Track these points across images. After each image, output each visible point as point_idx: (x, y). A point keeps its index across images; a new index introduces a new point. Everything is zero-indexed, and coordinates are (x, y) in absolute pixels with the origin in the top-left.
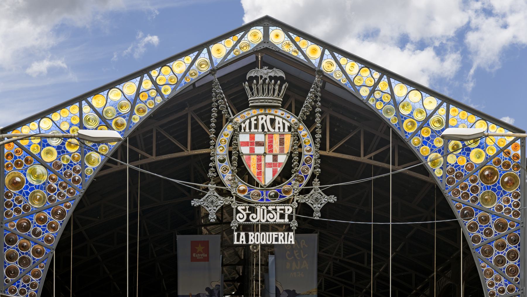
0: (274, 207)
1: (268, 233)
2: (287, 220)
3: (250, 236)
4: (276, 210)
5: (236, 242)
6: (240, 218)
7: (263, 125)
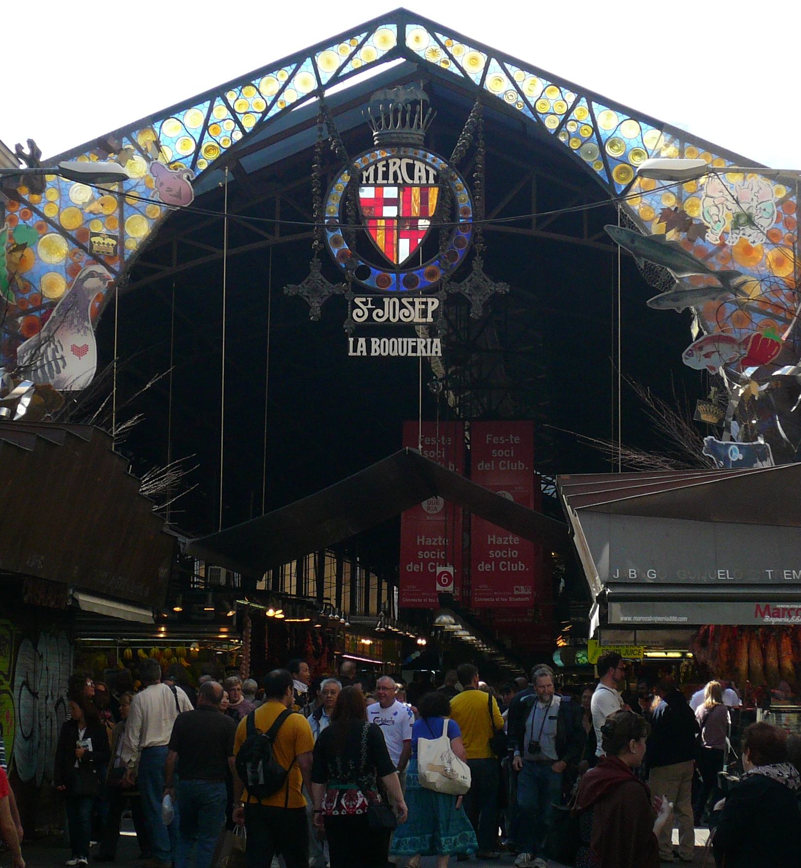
0: (411, 300)
2: (430, 319)
3: (373, 343)
4: (412, 304)
5: (351, 353)
6: (360, 315)
7: (395, 173)
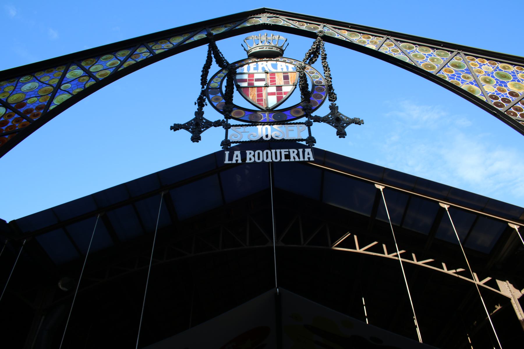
1: (274, 151)
5: (227, 161)
